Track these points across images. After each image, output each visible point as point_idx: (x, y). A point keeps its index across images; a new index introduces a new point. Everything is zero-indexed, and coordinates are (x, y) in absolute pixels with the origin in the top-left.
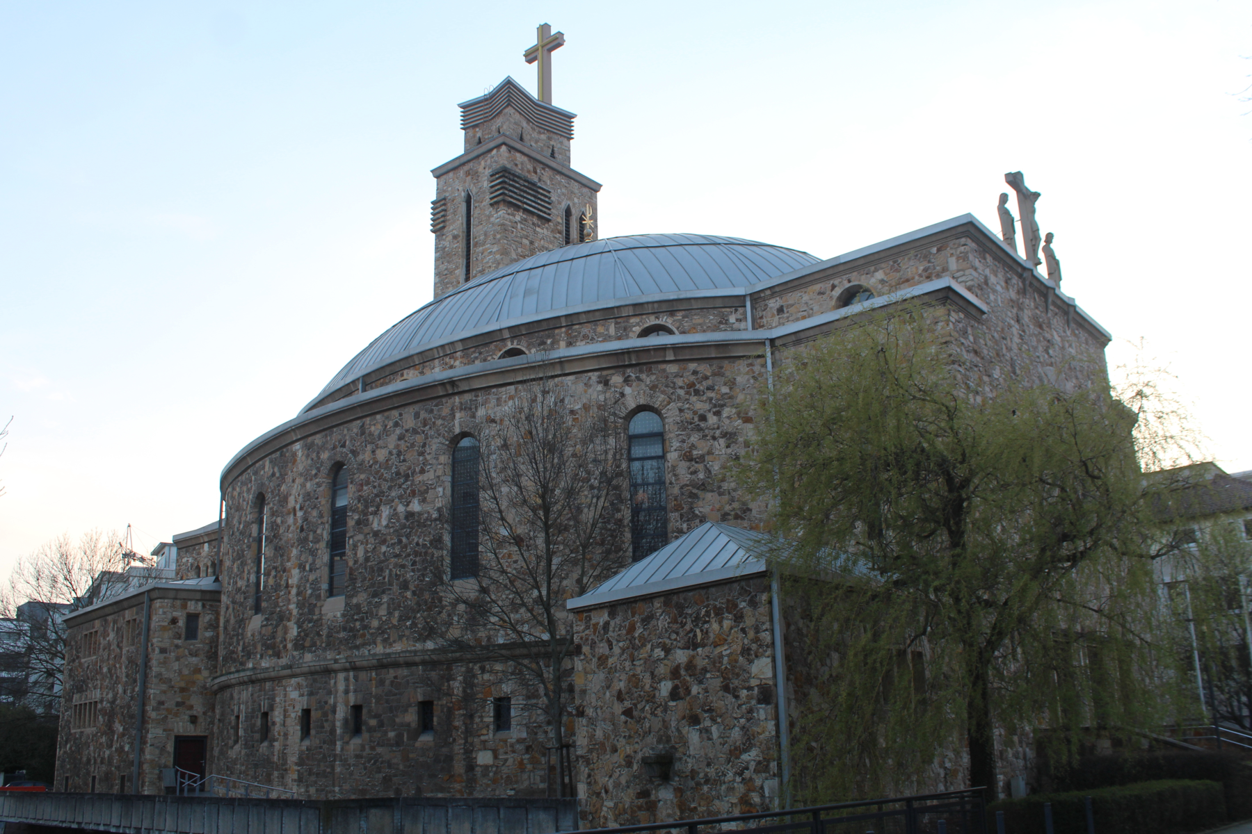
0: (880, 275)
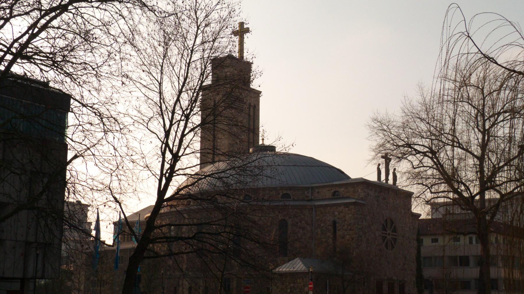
0: (343, 189)
